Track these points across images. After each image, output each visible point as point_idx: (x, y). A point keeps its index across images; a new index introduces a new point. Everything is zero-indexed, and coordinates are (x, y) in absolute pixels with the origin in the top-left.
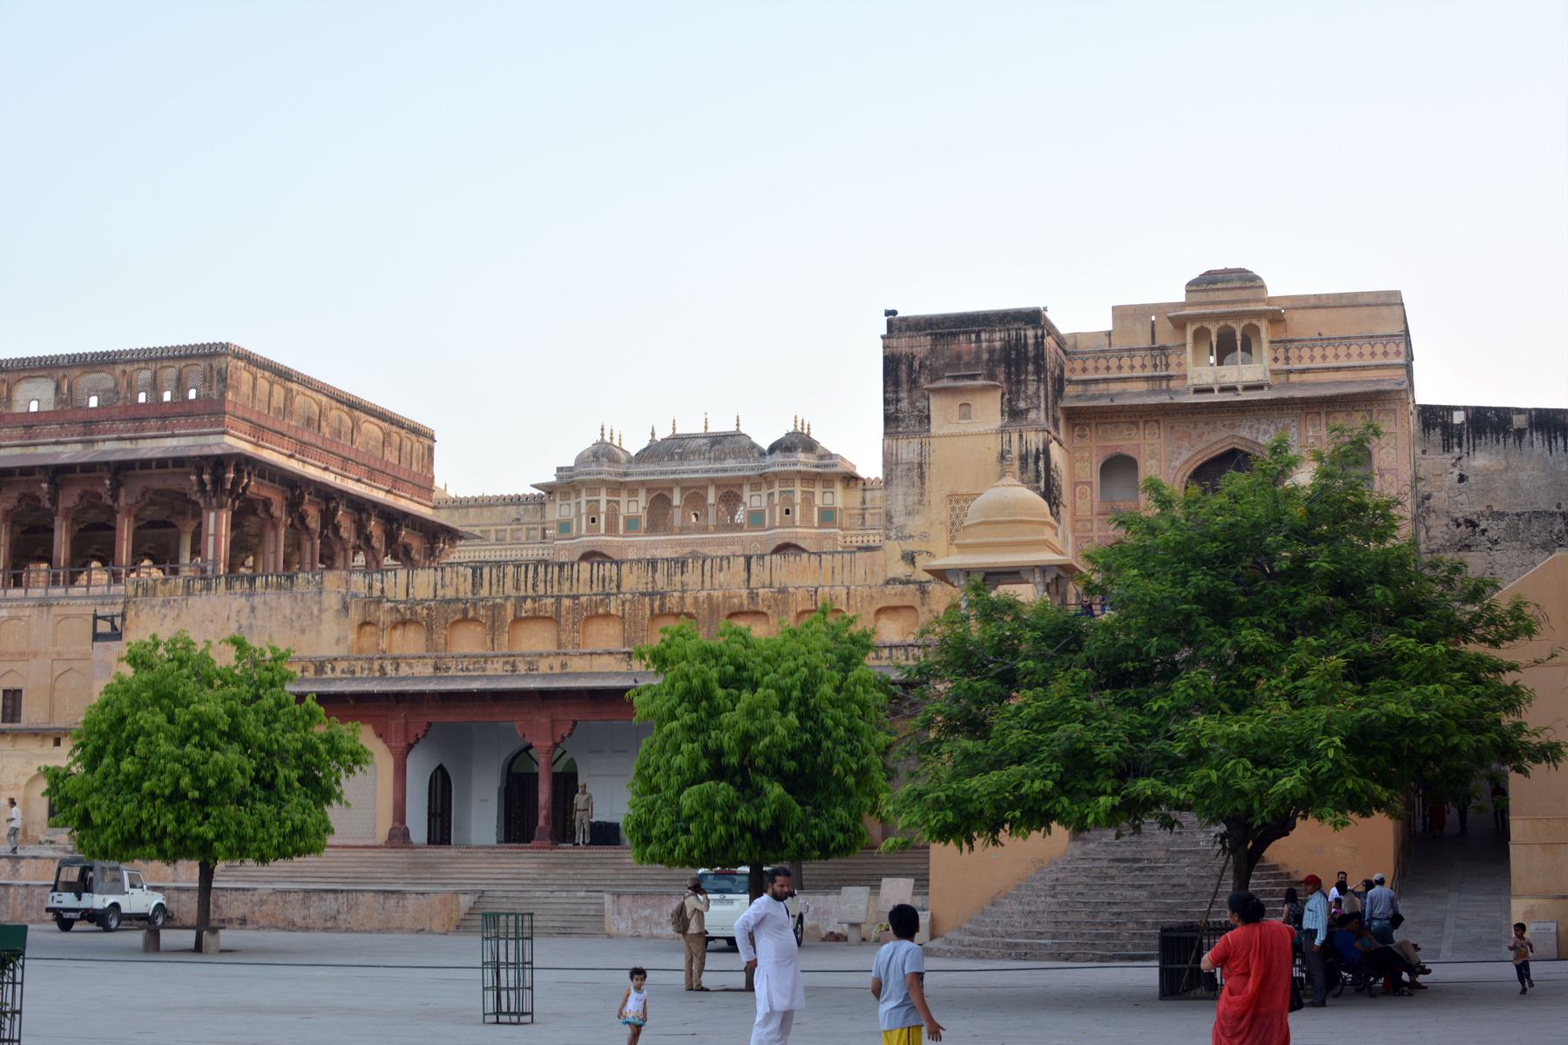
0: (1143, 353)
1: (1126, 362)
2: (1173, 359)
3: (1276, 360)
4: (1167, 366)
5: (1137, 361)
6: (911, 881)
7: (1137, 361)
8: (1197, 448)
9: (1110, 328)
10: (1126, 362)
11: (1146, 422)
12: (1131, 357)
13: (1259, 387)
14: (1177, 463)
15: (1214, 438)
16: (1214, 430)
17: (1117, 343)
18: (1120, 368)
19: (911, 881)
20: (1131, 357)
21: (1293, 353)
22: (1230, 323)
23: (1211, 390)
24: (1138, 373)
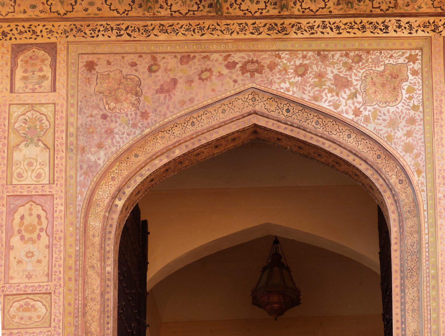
8: (155, 120)
14: (101, 158)
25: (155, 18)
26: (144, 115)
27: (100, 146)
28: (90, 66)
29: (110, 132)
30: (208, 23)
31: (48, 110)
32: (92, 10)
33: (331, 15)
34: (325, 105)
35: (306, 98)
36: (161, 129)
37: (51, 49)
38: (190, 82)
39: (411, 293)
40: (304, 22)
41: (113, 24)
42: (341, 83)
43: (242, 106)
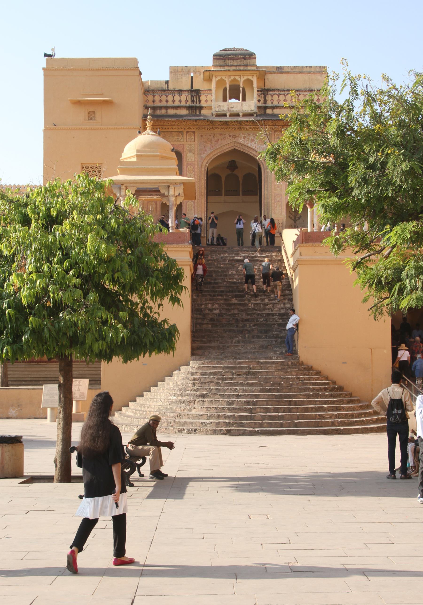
0: (186, 93)
1: (177, 98)
2: (203, 98)
3: (259, 101)
4: (200, 101)
5: (183, 98)
6: (87, 381)
7: (183, 98)
9: (168, 79)
10: (177, 98)
11: (187, 132)
12: (180, 95)
13: (251, 115)
14: (204, 156)
15: (224, 142)
16: (224, 138)
17: (171, 87)
18: (174, 101)
19: (87, 381)
20: (180, 95)
21: (269, 98)
22: (237, 78)
23: (225, 115)
24: (183, 104)
25: (215, 126)
26: (212, 147)
27: (204, 153)
28: (202, 136)
29: (206, 150)
30: (225, 127)
31: (193, 146)
32: (202, 124)
33: (251, 126)
34: (249, 145)
35: (245, 144)
36: (216, 150)
37: (194, 132)
38: (222, 139)
39: (266, 186)
40: (245, 127)
41: (206, 127)
42: (253, 140)
43: (232, 145)
